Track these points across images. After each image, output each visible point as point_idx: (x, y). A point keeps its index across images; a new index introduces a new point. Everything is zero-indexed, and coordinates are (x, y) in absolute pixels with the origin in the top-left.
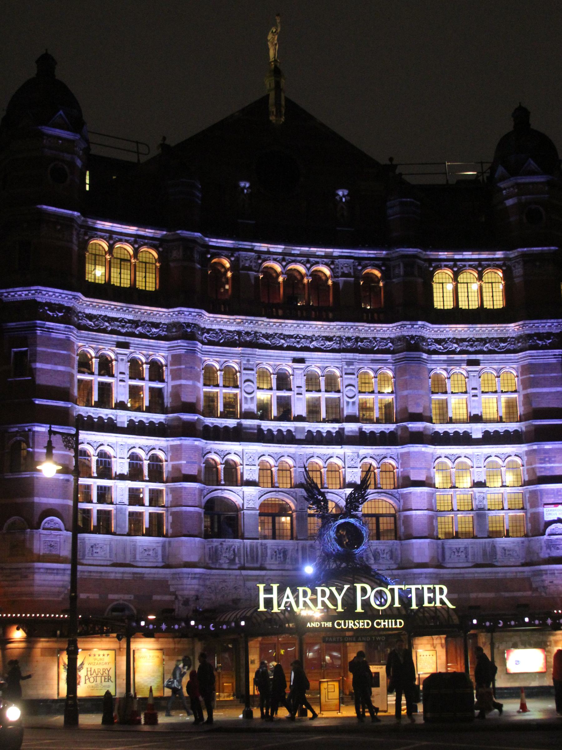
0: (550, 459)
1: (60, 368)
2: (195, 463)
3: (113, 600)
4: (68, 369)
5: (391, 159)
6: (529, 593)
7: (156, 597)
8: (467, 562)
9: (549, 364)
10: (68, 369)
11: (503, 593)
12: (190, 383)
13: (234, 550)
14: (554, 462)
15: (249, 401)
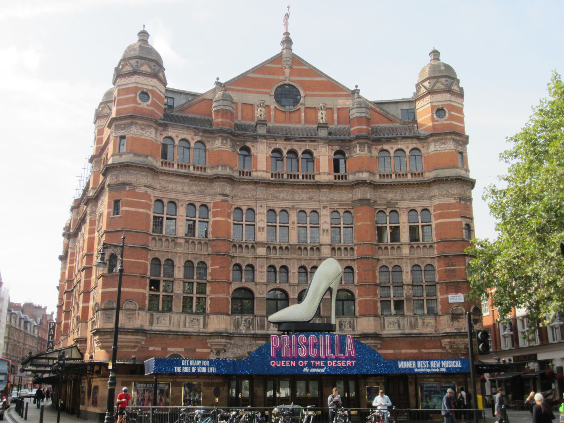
0: (452, 264)
1: (141, 210)
2: (225, 267)
3: (170, 352)
4: (146, 211)
5: (357, 86)
6: (440, 351)
7: (198, 350)
8: (400, 329)
9: (451, 204)
10: (146, 211)
11: (423, 350)
12: (224, 219)
13: (249, 321)
14: (455, 266)
15: (261, 230)
